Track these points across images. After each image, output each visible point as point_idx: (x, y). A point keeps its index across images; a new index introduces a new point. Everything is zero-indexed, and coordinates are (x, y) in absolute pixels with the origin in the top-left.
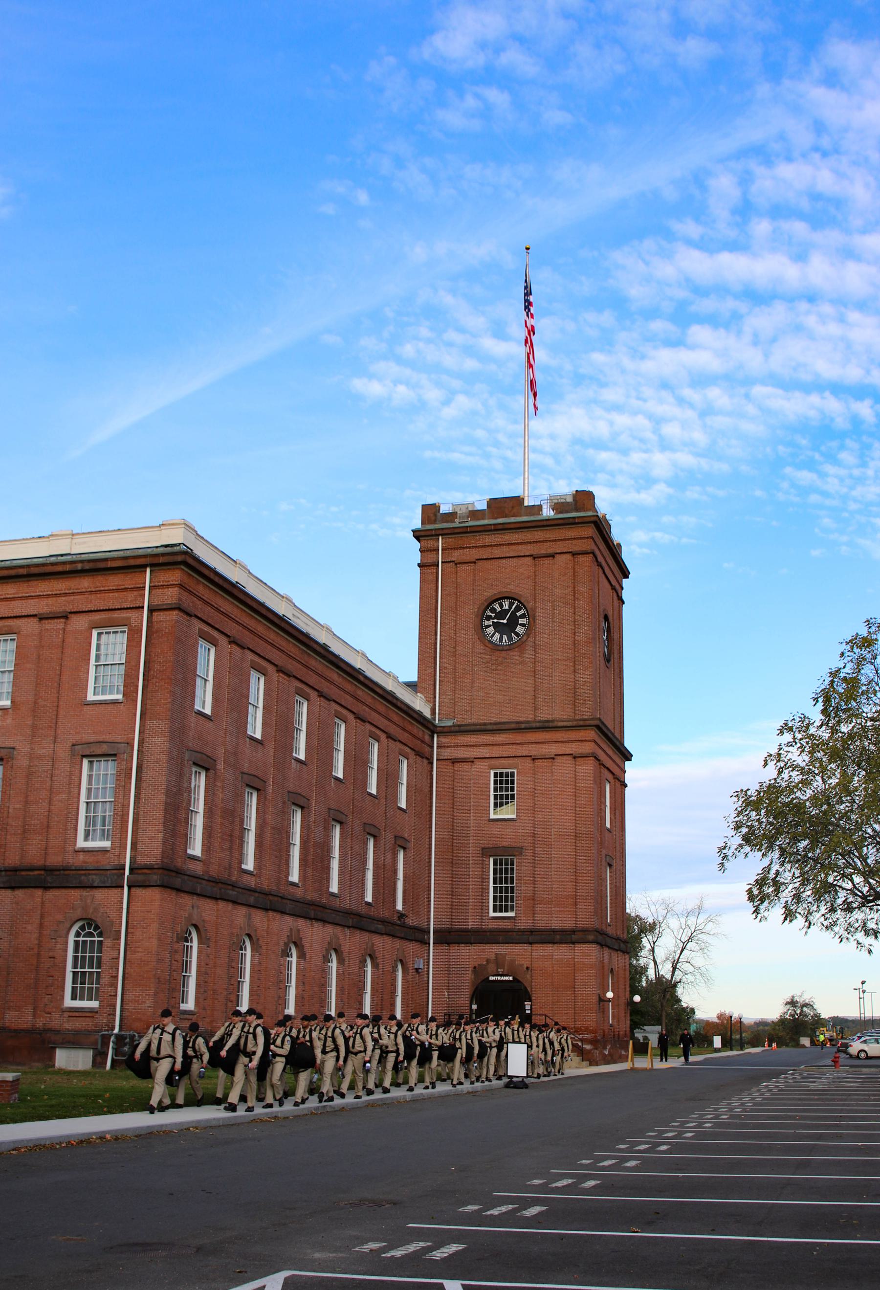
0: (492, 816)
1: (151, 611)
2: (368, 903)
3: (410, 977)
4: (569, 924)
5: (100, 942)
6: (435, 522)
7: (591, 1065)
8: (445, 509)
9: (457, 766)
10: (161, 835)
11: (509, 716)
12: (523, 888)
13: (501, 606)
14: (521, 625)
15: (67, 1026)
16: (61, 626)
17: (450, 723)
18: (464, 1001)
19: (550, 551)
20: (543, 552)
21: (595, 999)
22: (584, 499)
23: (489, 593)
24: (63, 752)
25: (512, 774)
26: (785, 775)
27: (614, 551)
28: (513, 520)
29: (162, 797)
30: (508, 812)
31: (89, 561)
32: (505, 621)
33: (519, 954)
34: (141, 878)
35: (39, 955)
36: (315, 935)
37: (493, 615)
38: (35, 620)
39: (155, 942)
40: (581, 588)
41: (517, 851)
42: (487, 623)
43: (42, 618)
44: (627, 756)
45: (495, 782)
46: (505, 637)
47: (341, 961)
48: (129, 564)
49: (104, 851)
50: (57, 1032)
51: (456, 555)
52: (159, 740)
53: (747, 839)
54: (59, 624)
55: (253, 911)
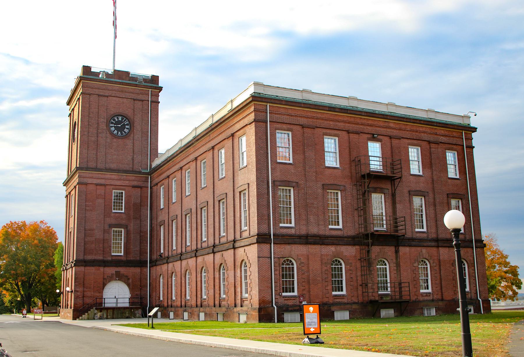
13: (118, 119)
42: (111, 125)
45: (122, 196)
46: (119, 133)
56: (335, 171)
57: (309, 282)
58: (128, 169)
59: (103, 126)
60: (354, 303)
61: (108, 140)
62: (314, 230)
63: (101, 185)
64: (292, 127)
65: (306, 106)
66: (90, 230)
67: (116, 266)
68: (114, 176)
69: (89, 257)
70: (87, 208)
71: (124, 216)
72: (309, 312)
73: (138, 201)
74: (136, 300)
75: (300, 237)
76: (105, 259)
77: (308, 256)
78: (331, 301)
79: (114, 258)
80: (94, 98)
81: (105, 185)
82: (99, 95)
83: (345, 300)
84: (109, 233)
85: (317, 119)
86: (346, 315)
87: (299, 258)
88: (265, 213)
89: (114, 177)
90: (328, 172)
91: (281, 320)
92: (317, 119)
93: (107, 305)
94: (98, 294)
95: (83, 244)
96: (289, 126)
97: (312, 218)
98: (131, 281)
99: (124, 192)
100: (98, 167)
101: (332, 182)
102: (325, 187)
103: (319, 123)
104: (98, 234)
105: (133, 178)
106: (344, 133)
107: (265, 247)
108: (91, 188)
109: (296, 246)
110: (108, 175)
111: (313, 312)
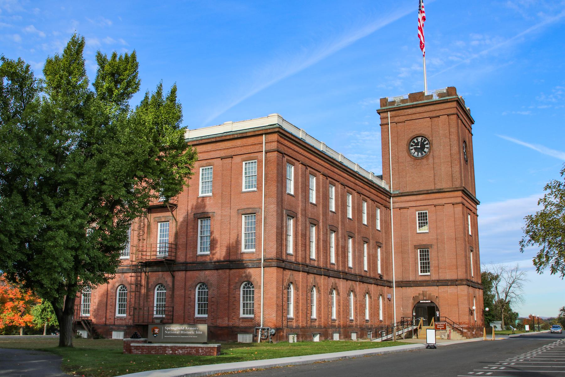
0: (418, 232)
1: (266, 153)
2: (365, 271)
3: (386, 302)
4: (454, 277)
5: (253, 291)
6: (386, 106)
7: (467, 338)
9: (402, 210)
10: (275, 246)
11: (423, 188)
12: (433, 262)
13: (417, 140)
15: (241, 325)
16: (230, 161)
17: (398, 192)
18: (409, 312)
19: (438, 115)
20: (434, 115)
21: (467, 310)
22: (451, 90)
23: (411, 135)
24: (234, 213)
25: (426, 213)
26: (548, 208)
27: (467, 113)
28: (420, 102)
29: (275, 230)
30: (425, 229)
31: (240, 134)
33: (433, 291)
34: (268, 264)
35: (229, 296)
36: (342, 284)
38: (220, 159)
39: (275, 290)
40: (452, 130)
41: (431, 246)
42: (411, 148)
43: (222, 158)
44: (477, 203)
45: (419, 217)
46: (420, 154)
47: (355, 296)
48: (256, 133)
49: (253, 253)
50: (238, 327)
51: (396, 119)
52: (272, 206)
53: (533, 238)
54: (229, 160)
55: (316, 276)
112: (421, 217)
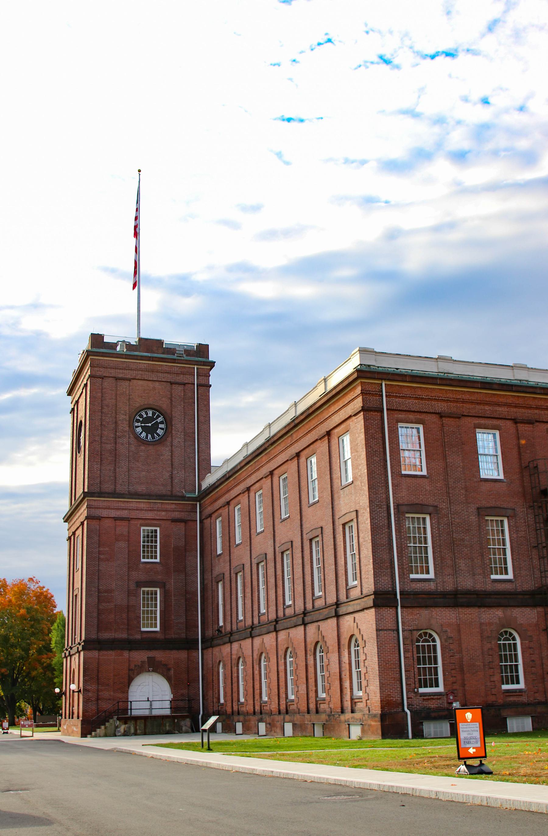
8: (106, 340)
13: (147, 414)
14: (160, 428)
32: (150, 425)
37: (141, 419)
42: (136, 424)
45: (156, 537)
46: (149, 436)
56: (497, 485)
57: (462, 670)
58: (164, 492)
59: (124, 426)
60: (540, 703)
61: (133, 448)
62: (467, 583)
63: (122, 519)
64: (423, 416)
65: (444, 382)
66: (106, 591)
67: (149, 649)
68: (143, 504)
69: (106, 635)
70: (102, 557)
71: (159, 568)
72: (465, 721)
73: (182, 543)
74: (181, 704)
75: (444, 595)
76: (131, 637)
77: (458, 625)
78: (500, 701)
79: (145, 636)
80: (107, 383)
81: (128, 519)
82: (117, 379)
83: (524, 699)
84: (137, 595)
85: (464, 402)
86: (527, 723)
87: (444, 629)
88: (386, 557)
89: (142, 506)
90: (485, 487)
91: (418, 734)
92: (464, 402)
93: (135, 713)
94: (120, 695)
95: (95, 615)
96: (418, 416)
97: (462, 564)
98: (172, 672)
99: (158, 529)
100: (118, 490)
101: (492, 503)
102: (482, 512)
103: (466, 408)
104: (120, 598)
105: (173, 506)
106: (509, 423)
107: (388, 612)
108: (107, 523)
109: (438, 609)
110: (134, 503)
111: (473, 720)
112: (148, 536)
